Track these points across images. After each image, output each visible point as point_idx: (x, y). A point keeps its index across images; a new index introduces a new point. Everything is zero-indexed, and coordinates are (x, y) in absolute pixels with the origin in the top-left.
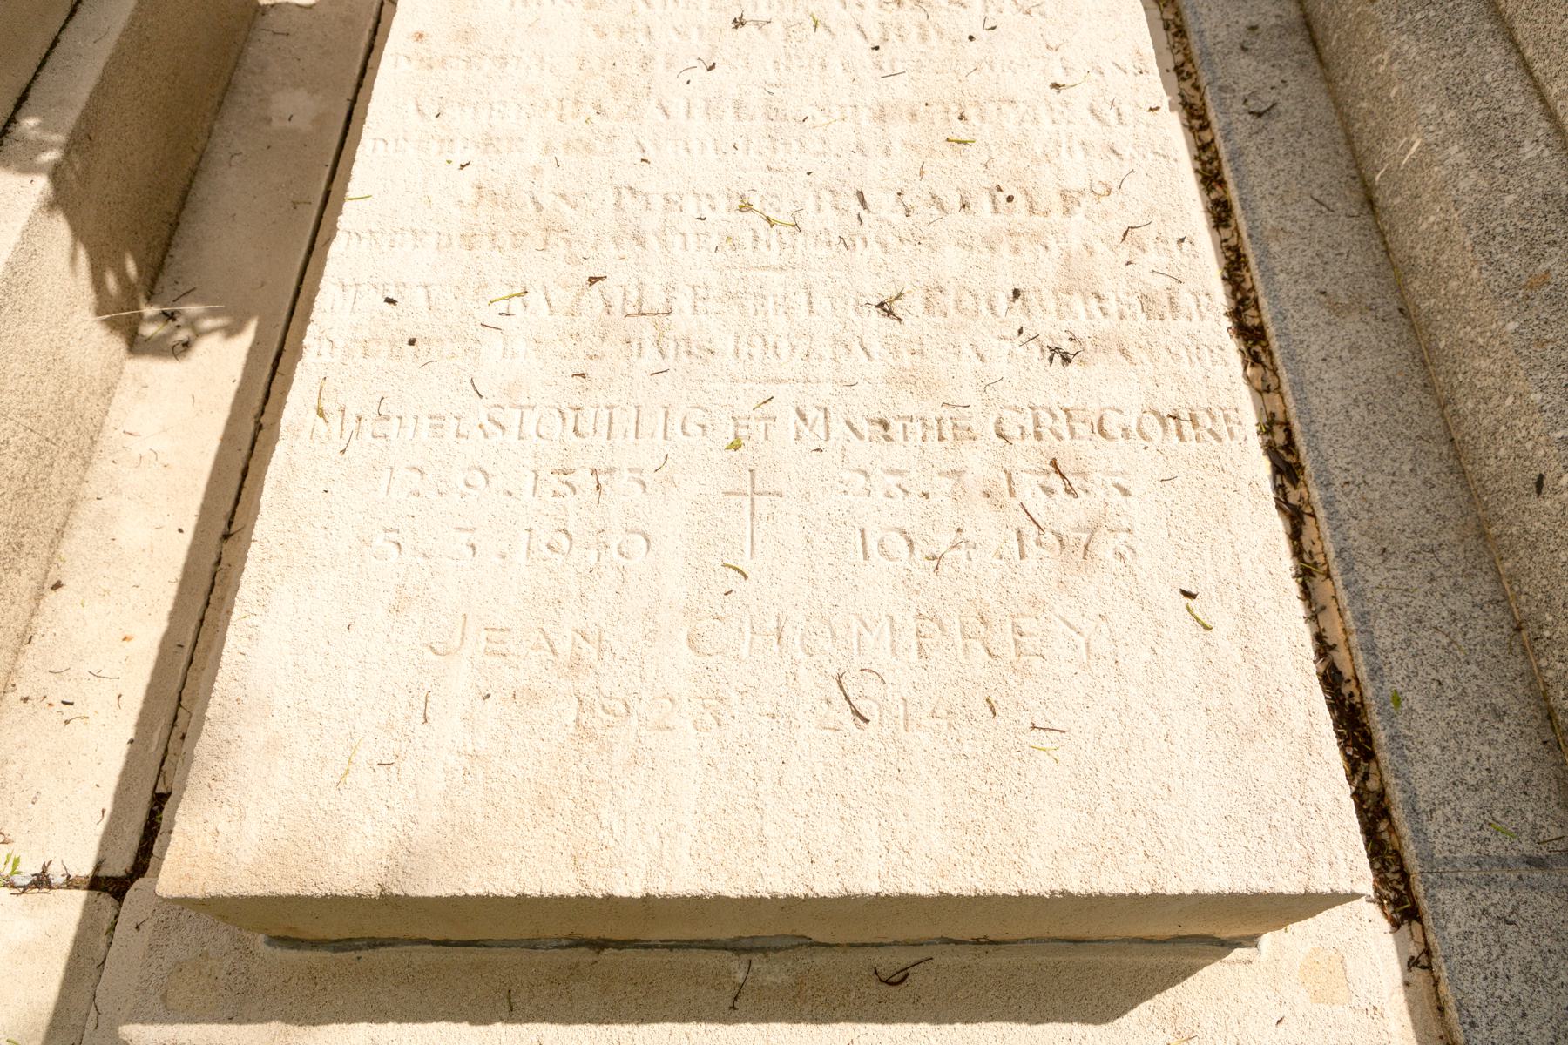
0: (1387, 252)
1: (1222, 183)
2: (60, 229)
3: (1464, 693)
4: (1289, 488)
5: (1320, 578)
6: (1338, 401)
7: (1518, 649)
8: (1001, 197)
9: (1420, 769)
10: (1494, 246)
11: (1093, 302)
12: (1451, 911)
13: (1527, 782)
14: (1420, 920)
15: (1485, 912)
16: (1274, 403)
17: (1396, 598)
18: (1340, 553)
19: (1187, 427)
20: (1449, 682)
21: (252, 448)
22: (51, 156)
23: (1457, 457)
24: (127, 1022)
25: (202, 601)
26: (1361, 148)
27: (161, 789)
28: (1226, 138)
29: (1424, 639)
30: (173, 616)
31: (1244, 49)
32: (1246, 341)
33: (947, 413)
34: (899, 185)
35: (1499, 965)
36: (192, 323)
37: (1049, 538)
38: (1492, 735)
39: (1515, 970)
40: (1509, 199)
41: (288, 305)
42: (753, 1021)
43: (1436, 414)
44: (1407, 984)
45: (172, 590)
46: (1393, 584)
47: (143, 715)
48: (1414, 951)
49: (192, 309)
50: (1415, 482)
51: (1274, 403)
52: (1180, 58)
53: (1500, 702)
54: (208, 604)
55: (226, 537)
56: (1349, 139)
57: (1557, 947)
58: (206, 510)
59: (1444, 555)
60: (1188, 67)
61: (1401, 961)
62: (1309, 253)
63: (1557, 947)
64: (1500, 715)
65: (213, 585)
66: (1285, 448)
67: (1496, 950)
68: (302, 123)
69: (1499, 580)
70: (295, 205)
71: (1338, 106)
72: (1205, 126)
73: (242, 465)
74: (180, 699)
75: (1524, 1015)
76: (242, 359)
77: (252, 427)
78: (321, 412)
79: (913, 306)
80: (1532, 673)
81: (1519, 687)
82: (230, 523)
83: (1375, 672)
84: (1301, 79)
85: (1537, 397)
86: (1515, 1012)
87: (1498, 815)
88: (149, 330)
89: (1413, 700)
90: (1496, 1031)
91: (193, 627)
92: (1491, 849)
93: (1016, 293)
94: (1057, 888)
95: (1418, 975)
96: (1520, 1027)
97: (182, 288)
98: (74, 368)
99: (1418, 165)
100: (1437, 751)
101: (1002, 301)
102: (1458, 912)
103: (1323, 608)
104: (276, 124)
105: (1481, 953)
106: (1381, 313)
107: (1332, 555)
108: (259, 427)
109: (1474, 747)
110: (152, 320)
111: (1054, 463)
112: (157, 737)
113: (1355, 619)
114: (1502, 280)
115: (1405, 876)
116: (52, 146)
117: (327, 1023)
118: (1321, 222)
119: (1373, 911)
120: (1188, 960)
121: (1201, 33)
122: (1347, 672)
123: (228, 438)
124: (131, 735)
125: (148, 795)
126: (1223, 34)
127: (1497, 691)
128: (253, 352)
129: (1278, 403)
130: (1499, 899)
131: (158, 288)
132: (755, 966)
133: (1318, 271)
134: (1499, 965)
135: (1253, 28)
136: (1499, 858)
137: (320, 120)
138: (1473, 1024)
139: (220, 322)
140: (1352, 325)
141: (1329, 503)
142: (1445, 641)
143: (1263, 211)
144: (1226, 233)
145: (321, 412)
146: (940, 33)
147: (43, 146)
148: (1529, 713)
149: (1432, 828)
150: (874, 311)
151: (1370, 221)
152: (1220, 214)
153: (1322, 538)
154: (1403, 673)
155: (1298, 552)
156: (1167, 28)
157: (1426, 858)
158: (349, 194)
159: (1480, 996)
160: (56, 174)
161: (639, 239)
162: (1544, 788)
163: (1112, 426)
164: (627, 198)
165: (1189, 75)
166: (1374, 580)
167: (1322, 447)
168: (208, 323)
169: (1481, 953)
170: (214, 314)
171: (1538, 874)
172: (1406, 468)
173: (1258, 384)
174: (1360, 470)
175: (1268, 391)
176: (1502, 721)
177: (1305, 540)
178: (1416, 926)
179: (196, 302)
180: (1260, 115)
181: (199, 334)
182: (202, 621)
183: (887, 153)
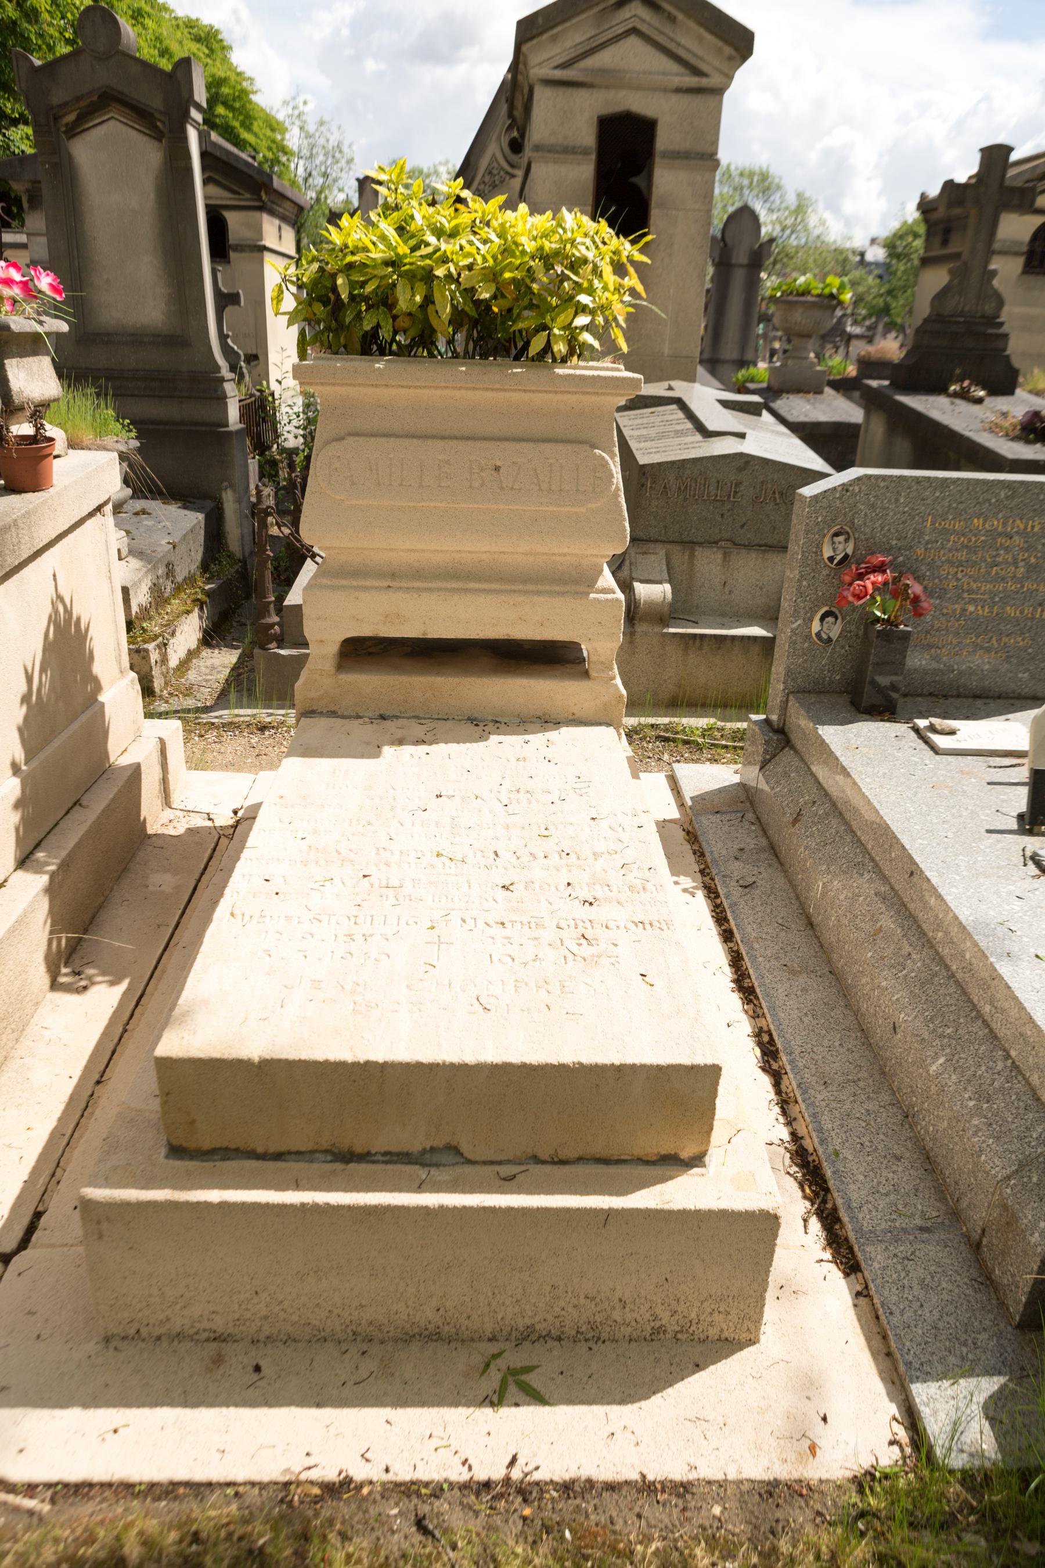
0: (822, 946)
1: (728, 921)
2: (44, 904)
3: (877, 1149)
4: (772, 1062)
5: (792, 1104)
6: (795, 1014)
7: (907, 1126)
8: (564, 854)
9: (852, 1187)
10: (858, 921)
11: (606, 888)
12: (875, 1258)
13: (917, 1190)
14: (861, 1271)
15: (895, 1255)
16: (762, 1022)
17: (834, 1104)
18: (799, 1085)
19: (648, 926)
20: (867, 1143)
21: (120, 1040)
22: (53, 868)
23: (866, 1038)
24: (86, 1186)
25: (79, 1114)
26: (803, 899)
27: (40, 1209)
28: (727, 898)
29: (852, 1123)
30: (60, 1120)
31: (737, 859)
32: (744, 994)
33: (533, 920)
34: (515, 849)
35: (906, 1282)
36: (90, 978)
37: (578, 958)
38: (895, 1168)
39: (915, 1283)
40: (861, 899)
41: (154, 962)
42: (430, 1192)
43: (853, 1018)
44: (855, 1306)
45: (62, 1107)
46: (832, 1098)
47: (35, 1168)
48: (859, 1288)
49: (91, 971)
50: (841, 1050)
51: (762, 1022)
52: (702, 867)
53: (899, 1152)
54: (82, 1116)
55: (98, 1082)
56: (798, 897)
57: (939, 1270)
58: (87, 1069)
59: (861, 1084)
60: (707, 871)
61: (851, 1293)
62: (776, 947)
63: (939, 1270)
64: (898, 1159)
65: (87, 1107)
66: (768, 1043)
67: (903, 1274)
68: (167, 888)
69: (894, 1093)
70: (159, 926)
71: (790, 882)
72: (718, 896)
73: (112, 1048)
74: (59, 1163)
75: (922, 1306)
76: (119, 997)
77: (121, 1030)
78: (232, 914)
79: (519, 888)
80: (916, 1137)
81: (909, 1145)
82: (102, 1076)
83: (822, 1141)
84: (770, 871)
85: (884, 984)
86: (916, 1305)
87: (900, 1207)
88: (62, 980)
89: (847, 1153)
90: (905, 1317)
91: (72, 1126)
92: (897, 1224)
93: (569, 884)
94: (576, 1061)
95: (862, 1301)
96: (920, 1312)
97: (85, 961)
98: (29, 981)
99: (824, 894)
100: (862, 1177)
101: (562, 886)
102: (879, 1257)
103: (795, 1119)
104: (151, 888)
105: (894, 1276)
106: (819, 973)
107: (795, 1087)
108: (125, 1031)
109: (884, 1174)
110: (66, 975)
111: (583, 936)
112: (42, 1181)
113: (810, 1116)
114: (863, 936)
115: (851, 1249)
116: (53, 864)
117: (196, 1189)
118: (783, 934)
119: (832, 1267)
120: (669, 1173)
121: (712, 852)
122: (811, 1150)
123: (105, 1034)
124: (26, 1178)
125: (31, 1212)
126: (724, 852)
127: (896, 1147)
128: (125, 994)
129: (764, 1022)
130: (903, 1249)
131: (71, 960)
132: (432, 1173)
133: (782, 955)
134: (906, 1282)
135: (742, 850)
136: (902, 1229)
137: (178, 888)
138: (891, 1313)
139: (106, 978)
140: (802, 980)
141: (791, 1062)
142: (864, 1124)
143: (749, 929)
144: (731, 945)
145: (232, 914)
146: (538, 801)
147: (48, 864)
148: (915, 1157)
149: (861, 1216)
150: (500, 889)
151: (811, 933)
152: (727, 936)
153: (790, 1082)
154: (840, 1140)
155: (778, 1092)
156: (694, 853)
157: (859, 1230)
158: (248, 845)
159: (894, 1298)
160: (53, 875)
161: (387, 865)
162: (927, 1192)
163: (611, 925)
164: (382, 851)
165: (708, 874)
166: (820, 1097)
167: (787, 1036)
168: (99, 979)
169: (894, 1276)
170: (103, 974)
171: (926, 1235)
172: (837, 1044)
173: (751, 1013)
174: (810, 1046)
175: (758, 1017)
176: (900, 1161)
177: (783, 1087)
178: (859, 1275)
179: (94, 968)
180: (746, 887)
181: (93, 984)
182: (78, 1124)
183: (509, 839)
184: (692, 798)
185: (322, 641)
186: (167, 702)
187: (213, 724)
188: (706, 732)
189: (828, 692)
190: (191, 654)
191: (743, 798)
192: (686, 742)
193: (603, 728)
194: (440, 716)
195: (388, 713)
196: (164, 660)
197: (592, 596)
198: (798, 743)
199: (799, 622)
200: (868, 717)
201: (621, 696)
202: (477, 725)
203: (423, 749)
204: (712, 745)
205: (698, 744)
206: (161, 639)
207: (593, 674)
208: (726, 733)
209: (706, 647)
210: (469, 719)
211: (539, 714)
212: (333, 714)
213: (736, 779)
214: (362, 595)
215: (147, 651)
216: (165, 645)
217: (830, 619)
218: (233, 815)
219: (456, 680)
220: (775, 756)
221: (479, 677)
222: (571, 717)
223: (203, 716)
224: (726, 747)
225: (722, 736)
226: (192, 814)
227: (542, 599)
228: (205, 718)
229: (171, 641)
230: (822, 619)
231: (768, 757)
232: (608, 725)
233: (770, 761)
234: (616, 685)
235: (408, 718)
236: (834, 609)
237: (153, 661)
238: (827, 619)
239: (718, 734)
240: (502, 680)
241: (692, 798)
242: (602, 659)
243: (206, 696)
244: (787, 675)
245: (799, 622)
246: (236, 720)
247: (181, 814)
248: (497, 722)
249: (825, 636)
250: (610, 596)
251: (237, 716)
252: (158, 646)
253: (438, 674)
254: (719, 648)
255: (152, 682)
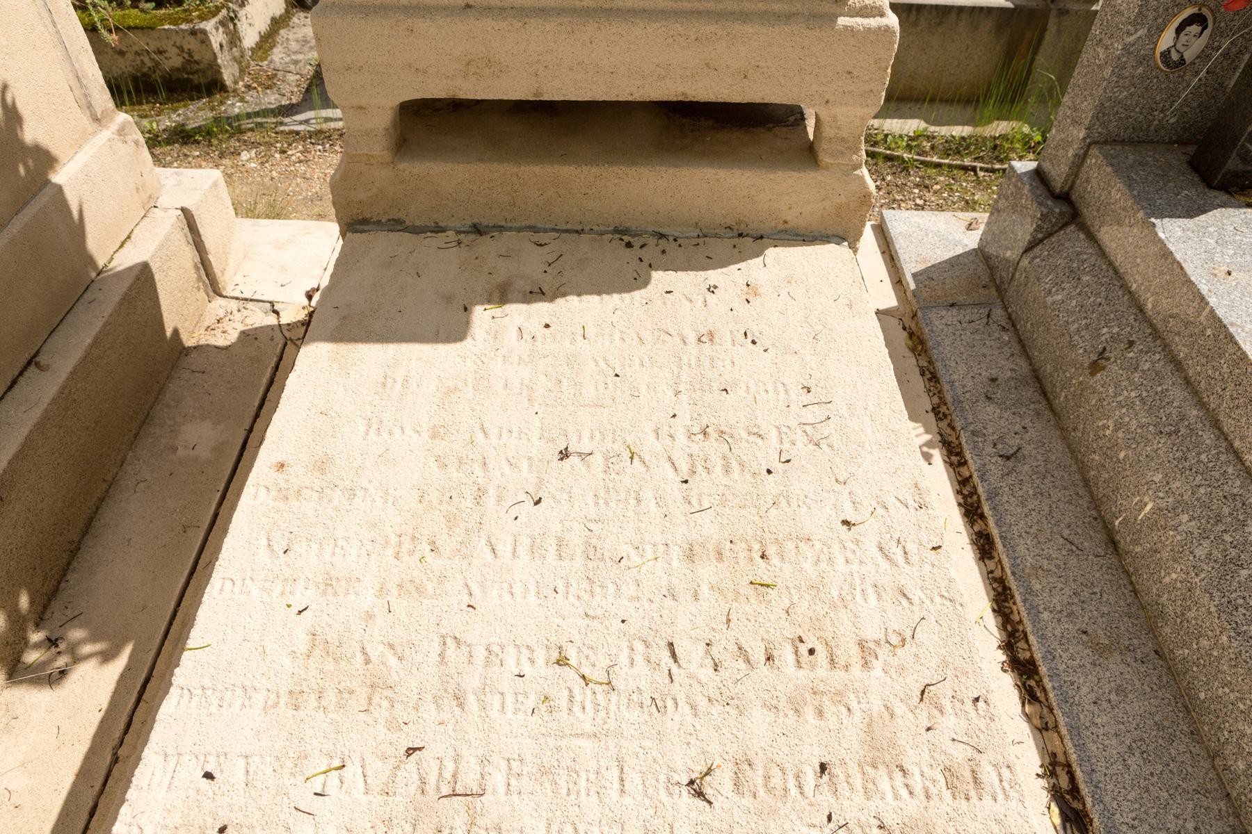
1: (982, 517)
8: (803, 649)
10: (1239, 616)
11: (898, 775)
26: (1100, 492)
28: (982, 478)
31: (988, 398)
34: (708, 635)
36: (72, 649)
43: (1207, 765)
49: (76, 634)
52: (936, 400)
56: (1086, 483)
60: (943, 409)
62: (1067, 591)
68: (204, 452)
70: (185, 528)
71: (1072, 452)
72: (963, 463)
76: (111, 686)
84: (1039, 425)
93: (823, 767)
99: (1152, 523)
101: (810, 777)
104: (181, 452)
108: (115, 760)
110: (37, 646)
118: (1073, 561)
121: (952, 383)
126: (970, 384)
128: (123, 677)
135: (993, 380)
137: (218, 449)
139: (98, 647)
140: (1114, 664)
143: (1021, 550)
144: (991, 564)
146: (741, 465)
150: (685, 790)
151: (1114, 560)
152: (984, 547)
156: (923, 374)
158: (191, 643)
164: (451, 652)
165: (945, 416)
167: (1107, 799)
168: (87, 649)
170: (93, 639)
173: (1037, 722)
175: (1047, 729)
179: (80, 626)
180: (1008, 458)
181: (77, 660)
183: (696, 597)
184: (914, 275)
185: (361, 108)
186: (242, 100)
187: (297, 133)
188: (913, 141)
189: (1151, 142)
190: (277, 24)
191: (985, 279)
192: (889, 158)
193: (831, 248)
194: (569, 227)
195: (485, 222)
196: (234, 39)
197: (842, 21)
198: (1088, 213)
199: (1141, 32)
200: (1225, 197)
201: (867, 195)
202: (629, 245)
203: (541, 310)
204: (922, 162)
205: (904, 161)
206: (224, 12)
207: (825, 158)
208: (937, 142)
209: (922, 21)
210: (616, 231)
211: (729, 223)
212: (396, 225)
213: (971, 241)
214: (421, 24)
215: (204, 32)
216: (232, 19)
217: (1195, 29)
218: (306, 302)
219: (595, 170)
220: (1050, 235)
221: (632, 163)
222: (781, 227)
223: (287, 120)
224: (938, 165)
225: (933, 148)
226: (250, 305)
227: (748, 29)
228: (293, 123)
229: (242, 13)
230: (1179, 30)
231: (1040, 236)
232: (839, 238)
233: (1041, 241)
234: (862, 178)
235: (519, 230)
236: (1205, 11)
237: (216, 46)
238: (1188, 29)
239: (927, 145)
240: (672, 170)
241: (914, 275)
242: (843, 134)
243: (291, 90)
244: (1096, 117)
245: (1141, 32)
246: (325, 126)
247: (234, 305)
248: (662, 236)
249: (1175, 56)
250: (873, 22)
251: (327, 120)
252: (222, 23)
253: (566, 157)
254: (940, 24)
255: (221, 73)
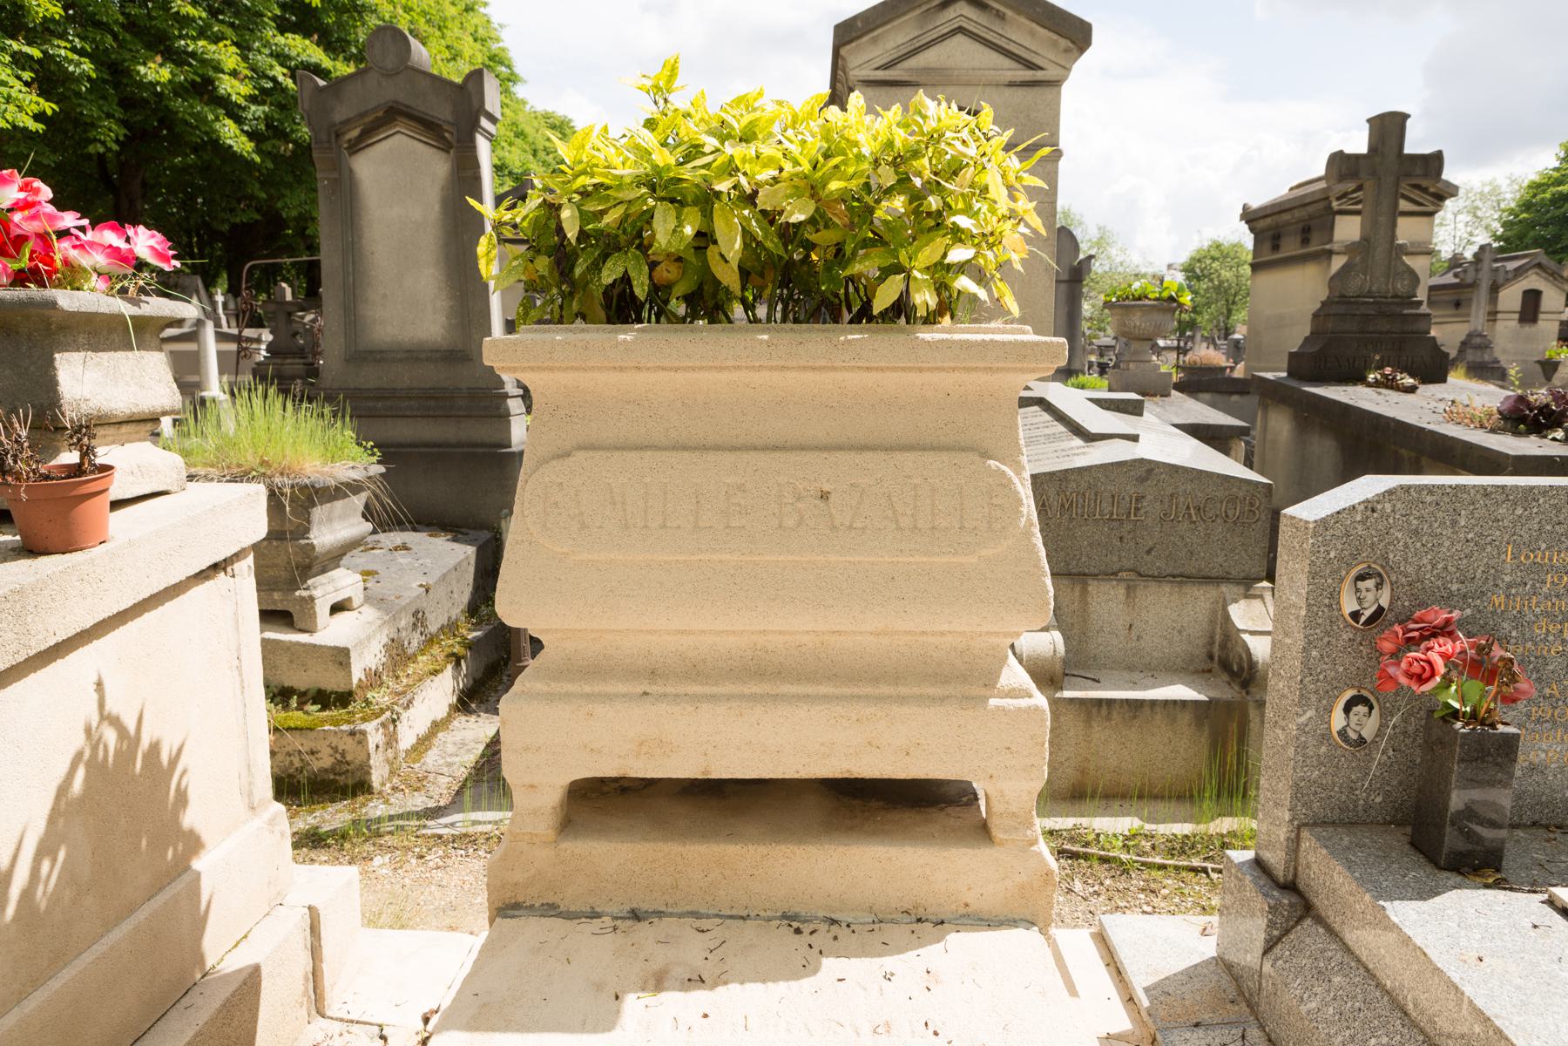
184: (1147, 990)
185: (532, 786)
186: (387, 802)
187: (440, 837)
188: (1129, 840)
189: (1364, 823)
190: (437, 727)
191: (1232, 992)
192: (1104, 860)
193: (1018, 933)
194: (734, 912)
195: (645, 907)
196: (391, 740)
197: (993, 702)
198: (1320, 902)
199: (1310, 713)
200: (1459, 879)
201: (1049, 873)
202: (798, 931)
203: (699, 998)
204: (1143, 864)
205: (1122, 863)
206: (388, 714)
207: (997, 833)
208: (1159, 841)
209: (1115, 715)
210: (785, 916)
211: (906, 906)
212: (551, 910)
213: (1208, 949)
214: (600, 709)
215: (363, 733)
216: (394, 721)
217: (1361, 709)
218: (421, 1024)
219: (762, 849)
220: (1287, 932)
221: (801, 842)
222: (962, 910)
223: (430, 823)
224: (1163, 867)
225: (1153, 847)
226: (355, 1028)
227: (905, 710)
228: (436, 827)
229: (404, 715)
230: (1347, 709)
231: (1276, 933)
232: (1030, 923)
233: (1279, 939)
234: (1040, 854)
235: (681, 916)
236: (1365, 693)
237: (372, 747)
238: (1355, 709)
239: (1147, 845)
240: (841, 849)
241: (1147, 990)
242: (1013, 808)
243: (441, 791)
244: (1295, 797)
245: (1310, 713)
246: (471, 830)
247: (337, 1027)
248: (833, 922)
249: (1353, 736)
250: (1023, 703)
251: (475, 823)
252: (383, 725)
253: (731, 837)
254: (1135, 717)
255: (369, 773)
